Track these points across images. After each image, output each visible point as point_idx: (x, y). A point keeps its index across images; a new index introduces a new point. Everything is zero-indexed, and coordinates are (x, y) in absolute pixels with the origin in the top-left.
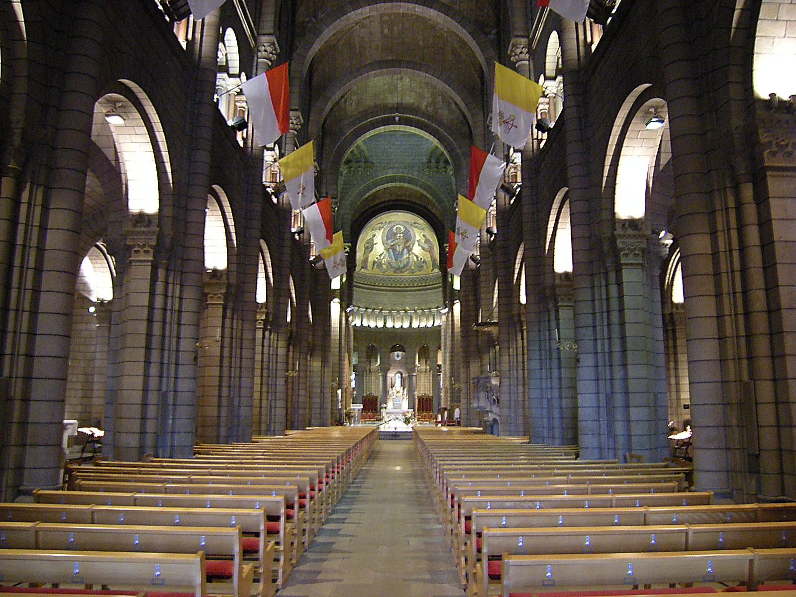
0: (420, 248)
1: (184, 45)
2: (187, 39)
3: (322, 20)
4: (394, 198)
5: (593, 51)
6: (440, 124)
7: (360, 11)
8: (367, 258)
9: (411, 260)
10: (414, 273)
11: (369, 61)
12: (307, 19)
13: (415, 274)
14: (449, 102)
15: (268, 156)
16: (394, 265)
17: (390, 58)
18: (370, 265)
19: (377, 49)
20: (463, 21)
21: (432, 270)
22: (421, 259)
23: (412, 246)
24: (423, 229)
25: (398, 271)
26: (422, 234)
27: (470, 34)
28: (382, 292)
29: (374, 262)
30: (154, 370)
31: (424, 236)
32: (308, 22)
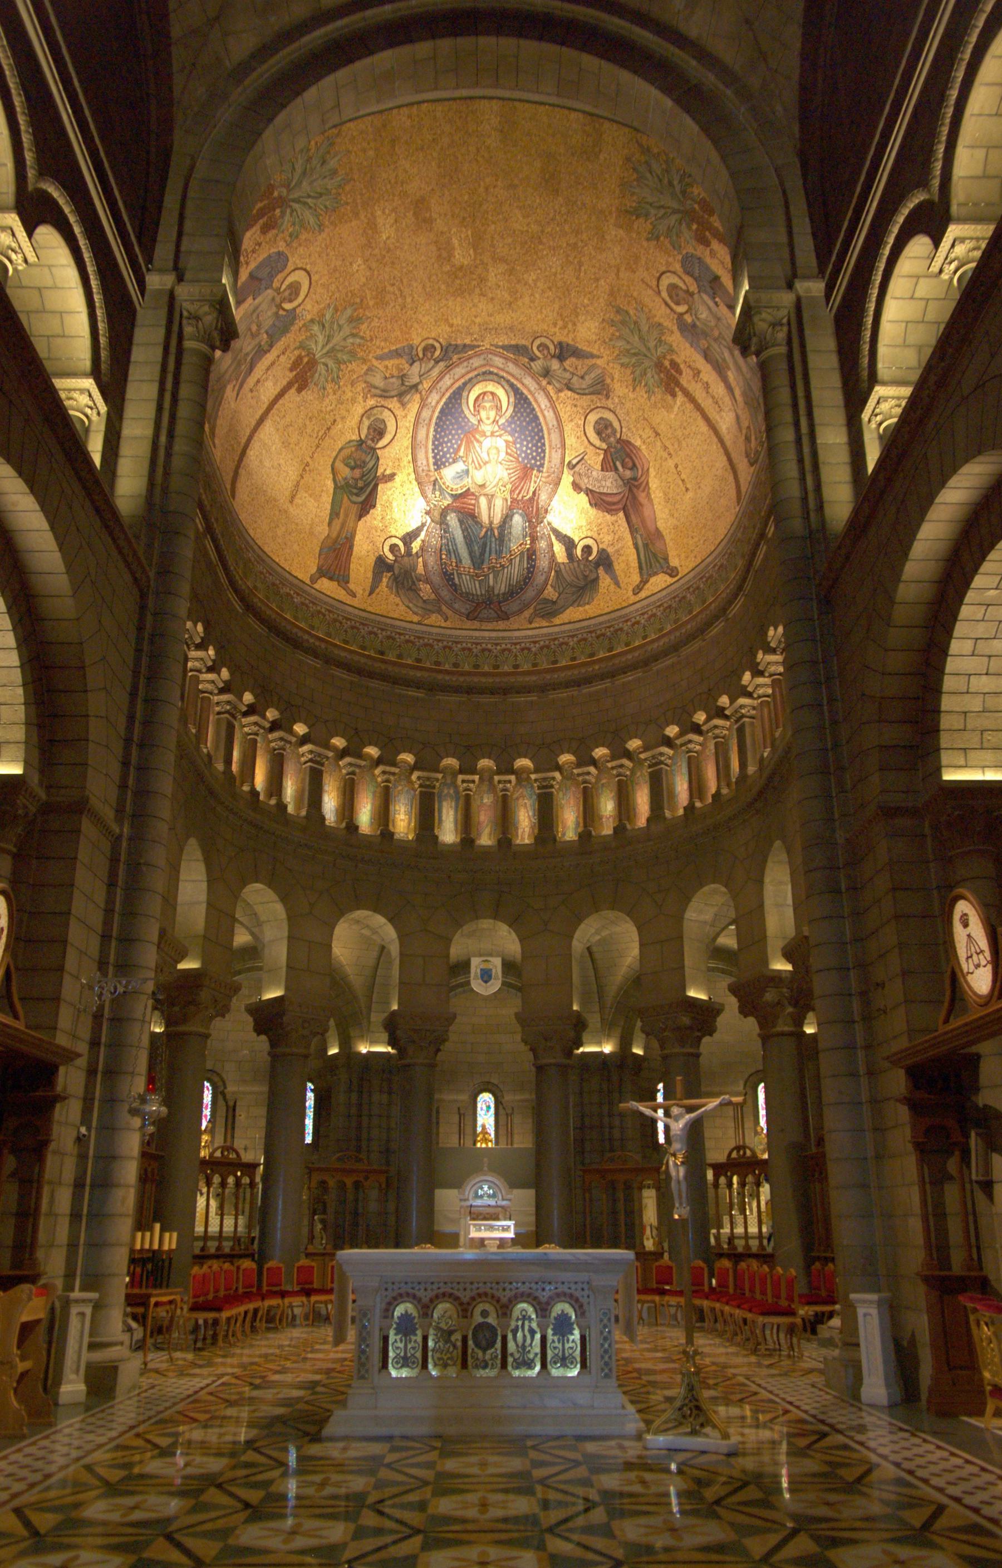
0: (583, 499)
8: (350, 540)
9: (543, 563)
10: (554, 614)
13: (557, 621)
16: (468, 584)
22: (587, 549)
23: (543, 497)
24: (600, 388)
25: (485, 614)
26: (593, 418)
28: (412, 693)
29: (381, 562)
31: (603, 429)
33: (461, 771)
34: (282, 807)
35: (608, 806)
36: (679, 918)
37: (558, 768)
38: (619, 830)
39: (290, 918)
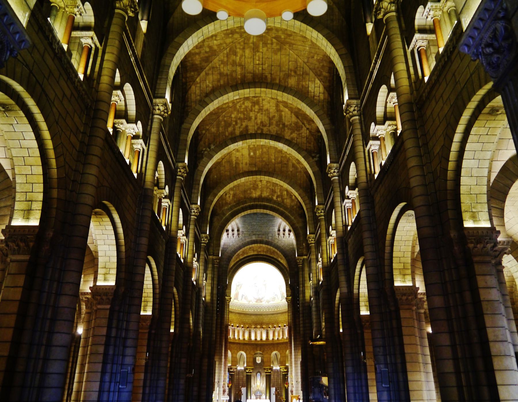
1: (135, 175)
2: (137, 172)
3: (213, 150)
4: (255, 253)
5: (375, 178)
6: (286, 208)
7: (236, 144)
8: (238, 293)
10: (268, 302)
11: (241, 172)
12: (204, 149)
13: (269, 303)
14: (291, 195)
15: (181, 233)
17: (254, 169)
18: (240, 297)
19: (246, 164)
20: (299, 150)
21: (281, 301)
27: (303, 157)
30: (107, 378)
32: (205, 151)
33: (255, 328)
34: (230, 338)
35: (276, 334)
36: (285, 353)
37: (269, 328)
38: (278, 339)
39: (232, 354)
